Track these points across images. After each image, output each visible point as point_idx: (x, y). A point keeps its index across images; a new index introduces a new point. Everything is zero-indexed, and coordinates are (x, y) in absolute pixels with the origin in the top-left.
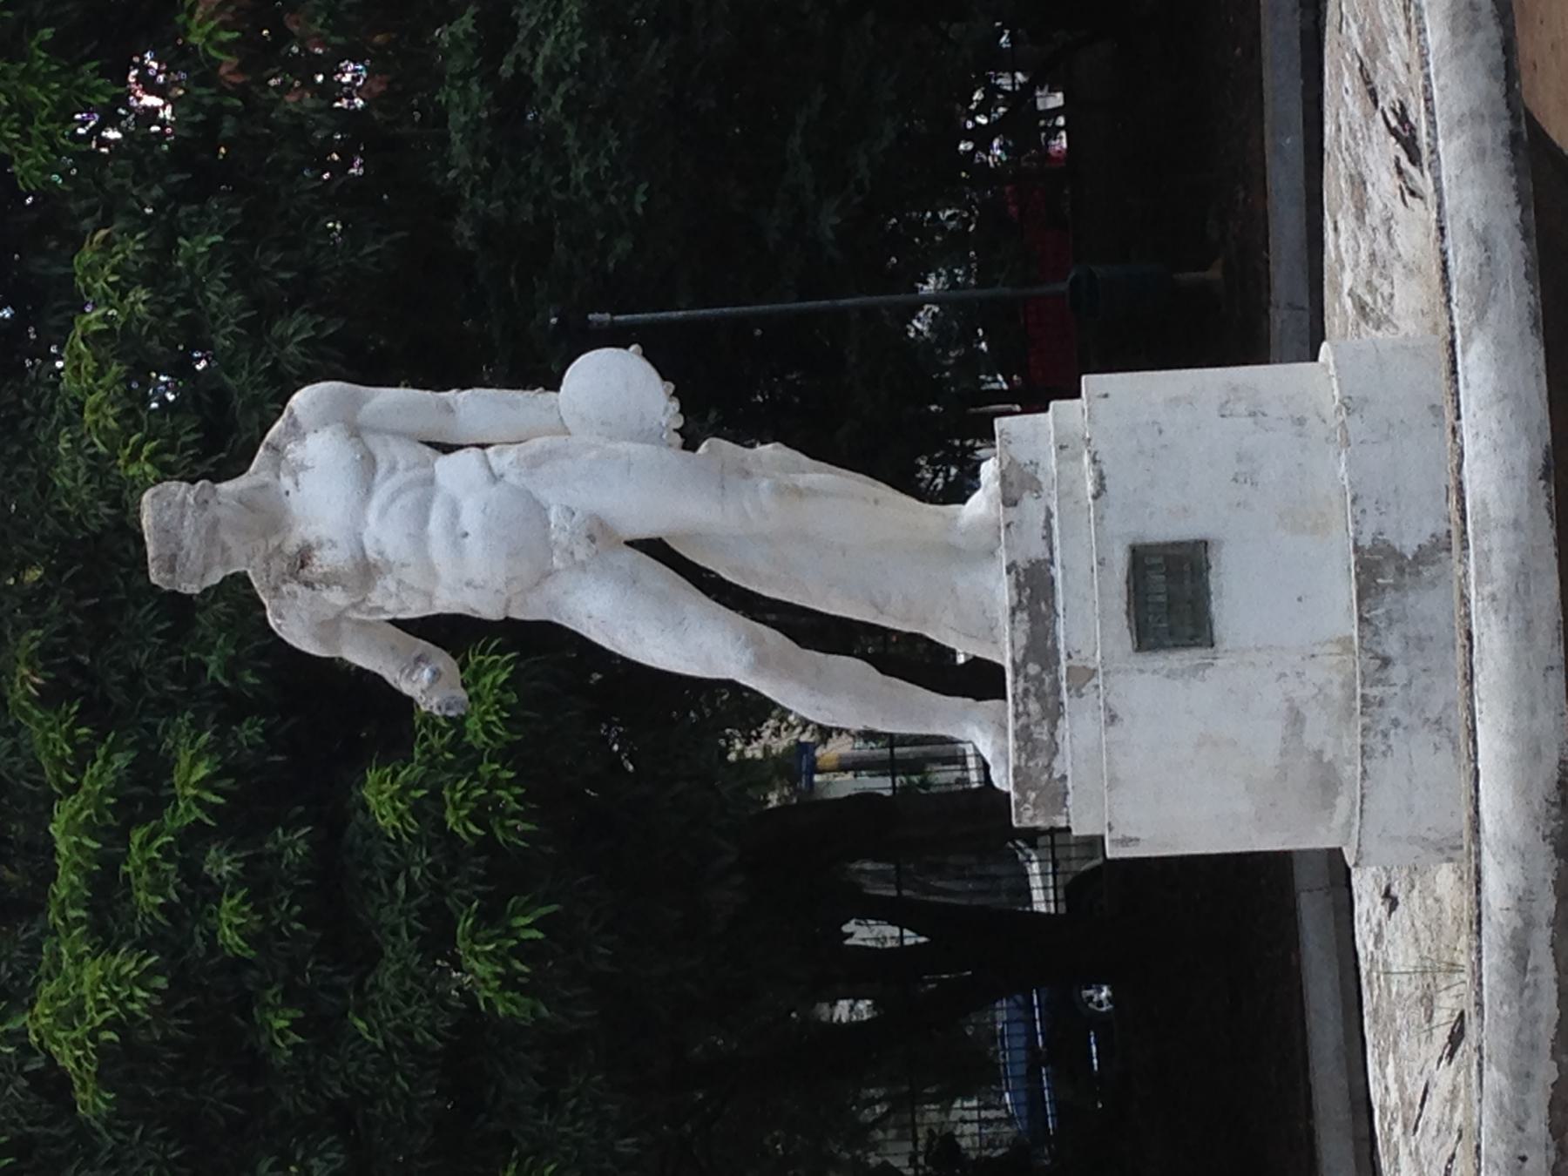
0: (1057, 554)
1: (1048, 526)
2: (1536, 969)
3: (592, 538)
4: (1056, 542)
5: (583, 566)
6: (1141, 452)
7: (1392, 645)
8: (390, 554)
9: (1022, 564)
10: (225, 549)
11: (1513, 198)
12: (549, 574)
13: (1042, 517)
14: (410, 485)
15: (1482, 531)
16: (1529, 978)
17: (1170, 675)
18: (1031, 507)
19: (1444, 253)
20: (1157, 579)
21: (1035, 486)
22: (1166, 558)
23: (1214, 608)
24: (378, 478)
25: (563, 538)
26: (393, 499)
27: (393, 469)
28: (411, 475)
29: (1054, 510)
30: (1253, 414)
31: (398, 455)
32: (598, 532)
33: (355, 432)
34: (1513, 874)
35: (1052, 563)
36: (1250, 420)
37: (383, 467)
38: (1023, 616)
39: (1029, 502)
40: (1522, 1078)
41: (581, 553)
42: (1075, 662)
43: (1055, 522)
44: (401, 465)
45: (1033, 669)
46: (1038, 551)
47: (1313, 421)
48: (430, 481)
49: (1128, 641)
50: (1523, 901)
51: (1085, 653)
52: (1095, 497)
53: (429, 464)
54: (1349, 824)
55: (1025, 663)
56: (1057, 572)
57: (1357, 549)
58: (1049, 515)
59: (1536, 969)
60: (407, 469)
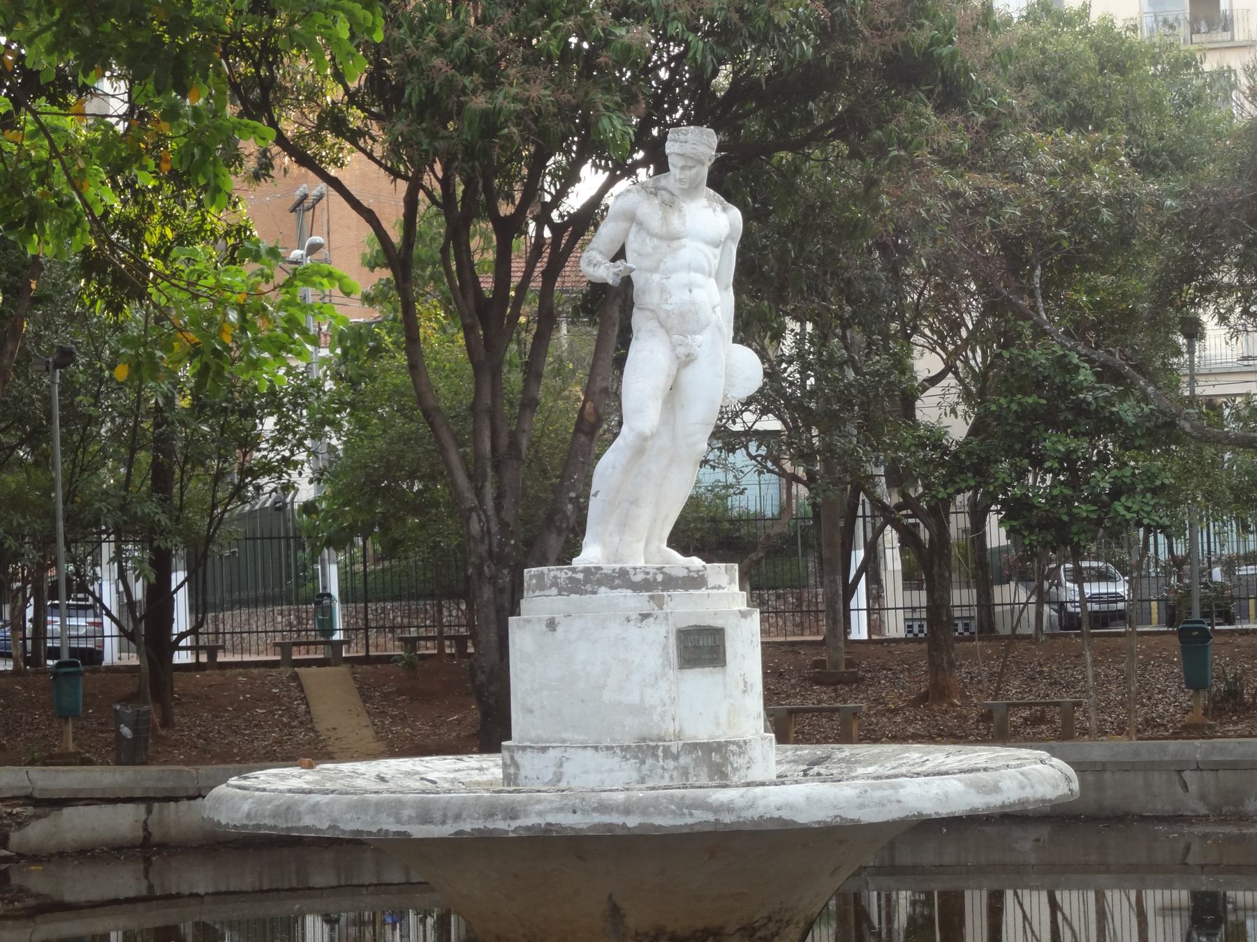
1: (720, 587)
2: (691, 814)
3: (688, 356)
4: (715, 591)
7: (684, 760)
8: (682, 252)
10: (691, 168)
12: (668, 332)
15: (893, 787)
16: (686, 811)
17: (665, 648)
20: (707, 641)
25: (689, 340)
26: (706, 256)
32: (686, 361)
34: (740, 803)
38: (684, 573)
40: (627, 810)
41: (681, 351)
42: (667, 599)
45: (660, 578)
46: (711, 583)
49: (683, 624)
50: (728, 808)
51: (671, 604)
54: (564, 741)
55: (664, 573)
56: (703, 591)
57: (727, 742)
59: (691, 814)
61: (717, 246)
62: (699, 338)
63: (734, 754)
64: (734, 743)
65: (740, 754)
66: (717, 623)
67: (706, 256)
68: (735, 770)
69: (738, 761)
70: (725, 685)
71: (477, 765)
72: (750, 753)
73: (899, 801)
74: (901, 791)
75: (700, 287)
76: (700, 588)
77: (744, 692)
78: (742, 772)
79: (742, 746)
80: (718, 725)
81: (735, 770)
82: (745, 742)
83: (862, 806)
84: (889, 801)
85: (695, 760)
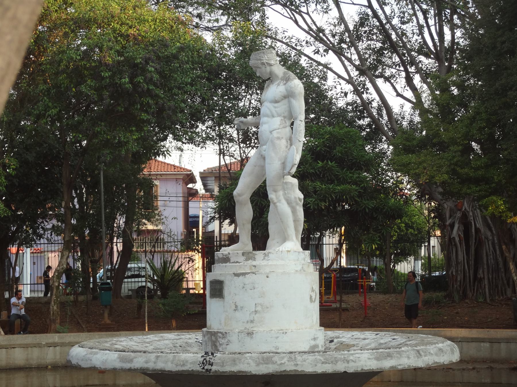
0: (231, 264)
1: (237, 262)
4: (233, 264)
5: (260, 154)
6: (245, 284)
9: (230, 256)
11: (136, 368)
13: (239, 261)
14: (271, 112)
18: (242, 259)
19: (141, 352)
21: (247, 260)
22: (221, 289)
23: (214, 299)
24: (273, 104)
26: (268, 108)
27: (275, 107)
28: (274, 112)
29: (240, 264)
30: (256, 312)
31: (282, 107)
33: (285, 97)
35: (230, 263)
36: (254, 310)
37: (276, 105)
39: (243, 258)
43: (238, 264)
44: (277, 109)
47: (252, 325)
48: (273, 116)
52: (234, 274)
53: (279, 115)
56: (228, 264)
58: (239, 263)
60: (276, 111)
61: (276, 102)
62: (264, 147)
63: (220, 338)
64: (220, 332)
65: (223, 338)
66: (221, 278)
67: (268, 108)
68: (221, 345)
69: (222, 341)
70: (224, 306)
71: (363, 336)
72: (228, 338)
73: (91, 360)
74: (95, 356)
75: (265, 123)
76: (227, 263)
77: (235, 310)
78: (224, 346)
79: (224, 335)
80: (221, 324)
81: (221, 345)
82: (226, 333)
83: (82, 360)
84: (89, 359)
85: (208, 338)
